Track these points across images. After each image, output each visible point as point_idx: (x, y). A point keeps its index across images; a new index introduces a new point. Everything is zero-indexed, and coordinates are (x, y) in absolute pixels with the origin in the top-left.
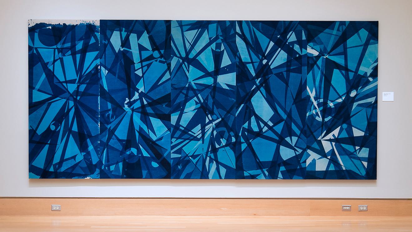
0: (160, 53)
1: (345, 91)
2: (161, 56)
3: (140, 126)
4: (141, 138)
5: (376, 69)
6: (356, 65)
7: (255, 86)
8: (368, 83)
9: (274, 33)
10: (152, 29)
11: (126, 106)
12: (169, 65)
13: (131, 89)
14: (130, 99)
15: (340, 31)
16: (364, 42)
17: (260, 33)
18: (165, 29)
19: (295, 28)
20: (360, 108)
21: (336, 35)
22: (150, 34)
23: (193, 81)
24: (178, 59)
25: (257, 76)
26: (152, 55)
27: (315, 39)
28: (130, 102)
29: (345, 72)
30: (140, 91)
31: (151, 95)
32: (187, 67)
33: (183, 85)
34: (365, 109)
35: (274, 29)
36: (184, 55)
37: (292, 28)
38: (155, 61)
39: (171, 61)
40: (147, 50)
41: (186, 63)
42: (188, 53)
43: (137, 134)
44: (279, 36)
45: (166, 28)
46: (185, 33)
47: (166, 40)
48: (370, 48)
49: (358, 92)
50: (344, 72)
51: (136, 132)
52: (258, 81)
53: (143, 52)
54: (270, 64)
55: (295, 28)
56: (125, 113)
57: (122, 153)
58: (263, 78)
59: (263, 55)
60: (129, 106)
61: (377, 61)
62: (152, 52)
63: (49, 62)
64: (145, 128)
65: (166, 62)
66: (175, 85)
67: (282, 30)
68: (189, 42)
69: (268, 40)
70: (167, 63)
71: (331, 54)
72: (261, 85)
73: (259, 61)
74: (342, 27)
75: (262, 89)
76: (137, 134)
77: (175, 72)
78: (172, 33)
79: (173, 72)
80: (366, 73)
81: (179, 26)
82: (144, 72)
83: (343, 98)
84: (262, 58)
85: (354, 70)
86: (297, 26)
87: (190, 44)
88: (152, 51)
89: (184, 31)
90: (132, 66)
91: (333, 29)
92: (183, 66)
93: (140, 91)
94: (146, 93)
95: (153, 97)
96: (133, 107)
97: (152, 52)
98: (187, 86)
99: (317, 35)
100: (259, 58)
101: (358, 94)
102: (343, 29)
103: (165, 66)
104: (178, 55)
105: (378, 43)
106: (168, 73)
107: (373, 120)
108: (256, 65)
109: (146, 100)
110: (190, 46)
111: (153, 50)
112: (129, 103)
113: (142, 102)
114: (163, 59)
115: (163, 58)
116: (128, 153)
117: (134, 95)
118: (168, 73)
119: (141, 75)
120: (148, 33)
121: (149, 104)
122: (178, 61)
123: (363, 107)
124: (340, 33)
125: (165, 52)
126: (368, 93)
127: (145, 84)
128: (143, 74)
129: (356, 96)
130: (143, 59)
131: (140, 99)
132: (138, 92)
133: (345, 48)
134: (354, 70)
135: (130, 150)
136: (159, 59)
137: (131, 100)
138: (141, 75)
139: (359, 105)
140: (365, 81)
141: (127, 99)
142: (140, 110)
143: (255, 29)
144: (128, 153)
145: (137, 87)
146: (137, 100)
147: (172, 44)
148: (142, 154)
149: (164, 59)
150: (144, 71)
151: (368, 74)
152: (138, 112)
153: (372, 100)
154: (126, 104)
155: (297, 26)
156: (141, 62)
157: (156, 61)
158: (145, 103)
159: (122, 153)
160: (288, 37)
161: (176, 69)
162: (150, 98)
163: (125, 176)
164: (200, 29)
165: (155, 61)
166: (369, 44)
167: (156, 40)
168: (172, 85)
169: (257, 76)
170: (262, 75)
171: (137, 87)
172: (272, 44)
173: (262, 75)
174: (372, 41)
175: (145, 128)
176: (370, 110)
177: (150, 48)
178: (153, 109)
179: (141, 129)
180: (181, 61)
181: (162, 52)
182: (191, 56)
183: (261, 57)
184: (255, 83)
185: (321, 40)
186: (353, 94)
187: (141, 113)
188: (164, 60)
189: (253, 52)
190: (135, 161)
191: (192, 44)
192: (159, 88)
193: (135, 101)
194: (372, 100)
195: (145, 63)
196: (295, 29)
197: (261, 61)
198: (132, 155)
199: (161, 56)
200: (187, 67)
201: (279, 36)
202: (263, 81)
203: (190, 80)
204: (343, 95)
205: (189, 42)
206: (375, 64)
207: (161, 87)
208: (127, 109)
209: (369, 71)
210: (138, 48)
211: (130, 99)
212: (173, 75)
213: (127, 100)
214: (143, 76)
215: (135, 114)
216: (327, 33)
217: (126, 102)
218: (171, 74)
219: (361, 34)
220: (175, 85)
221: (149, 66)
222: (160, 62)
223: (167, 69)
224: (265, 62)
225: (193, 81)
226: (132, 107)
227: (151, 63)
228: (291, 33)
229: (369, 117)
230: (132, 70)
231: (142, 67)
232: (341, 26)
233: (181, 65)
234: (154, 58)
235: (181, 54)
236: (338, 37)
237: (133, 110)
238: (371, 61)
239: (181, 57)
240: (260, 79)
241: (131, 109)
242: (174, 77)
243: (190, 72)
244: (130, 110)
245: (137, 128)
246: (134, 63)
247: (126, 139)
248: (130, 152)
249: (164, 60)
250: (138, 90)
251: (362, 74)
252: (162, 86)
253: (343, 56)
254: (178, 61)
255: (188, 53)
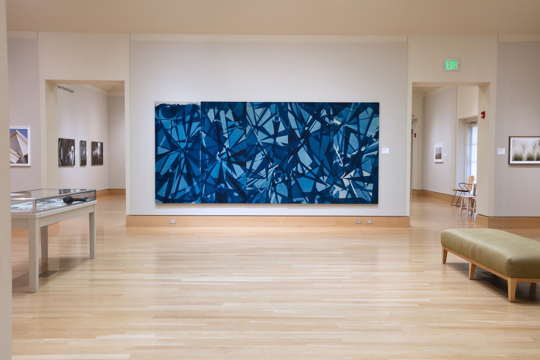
0: (239, 123)
3: (226, 170)
5: (377, 133)
7: (300, 144)
8: (372, 142)
11: (218, 157)
12: (245, 131)
13: (221, 146)
14: (220, 152)
21: (352, 112)
22: (233, 111)
23: (261, 140)
25: (302, 138)
26: (234, 124)
27: (339, 114)
30: (226, 148)
31: (234, 150)
33: (254, 143)
36: (254, 124)
40: (230, 121)
41: (256, 130)
42: (257, 123)
43: (225, 175)
44: (315, 112)
46: (256, 110)
48: (374, 120)
51: (224, 173)
52: (302, 141)
54: (310, 130)
56: (217, 161)
57: (215, 186)
59: (305, 124)
60: (220, 157)
61: (378, 128)
64: (230, 171)
65: (243, 129)
67: (318, 108)
71: (349, 123)
72: (304, 143)
73: (302, 128)
74: (356, 107)
75: (305, 146)
76: (225, 175)
77: (249, 135)
78: (247, 110)
80: (371, 136)
83: (357, 152)
85: (364, 134)
86: (327, 106)
87: (259, 117)
90: (221, 131)
92: (254, 131)
93: (226, 148)
98: (257, 144)
100: (303, 126)
103: (243, 131)
104: (251, 124)
105: (379, 116)
106: (244, 135)
107: (375, 166)
108: (301, 130)
111: (235, 121)
113: (228, 154)
114: (241, 127)
116: (219, 187)
118: (244, 135)
119: (227, 137)
121: (232, 156)
122: (251, 128)
123: (370, 157)
124: (355, 110)
125: (242, 122)
128: (229, 136)
129: (365, 150)
130: (228, 127)
131: (227, 152)
132: (225, 148)
133: (358, 120)
135: (220, 185)
136: (239, 127)
137: (221, 153)
138: (227, 137)
139: (367, 156)
141: (218, 152)
142: (227, 160)
143: (300, 108)
144: (219, 187)
145: (225, 144)
147: (247, 117)
148: (228, 187)
150: (229, 135)
151: (373, 137)
153: (375, 153)
154: (218, 155)
155: (327, 106)
156: (227, 128)
157: (237, 128)
158: (230, 155)
159: (215, 186)
161: (250, 133)
163: (217, 202)
164: (265, 108)
168: (247, 143)
169: (302, 138)
172: (311, 117)
174: (375, 115)
175: (230, 171)
176: (374, 159)
179: (227, 171)
180: (253, 128)
181: (241, 122)
182: (259, 125)
183: (304, 125)
184: (300, 143)
186: (363, 149)
188: (242, 128)
190: (223, 192)
193: (223, 154)
194: (375, 153)
195: (229, 130)
197: (304, 128)
199: (240, 125)
201: (315, 112)
203: (259, 140)
204: (356, 150)
206: (377, 130)
207: (240, 145)
209: (373, 135)
211: (220, 152)
213: (218, 153)
214: (228, 138)
216: (346, 110)
217: (217, 154)
218: (246, 136)
221: (232, 131)
222: (240, 128)
224: (306, 128)
225: (261, 140)
226: (221, 157)
227: (234, 129)
228: (323, 110)
229: (373, 164)
231: (228, 132)
233: (253, 131)
237: (222, 159)
238: (374, 128)
239: (253, 126)
240: (303, 140)
242: (248, 138)
244: (220, 160)
245: (225, 171)
249: (242, 128)
250: (225, 147)
251: (369, 136)
252: (241, 144)
253: (357, 125)
255: (257, 123)
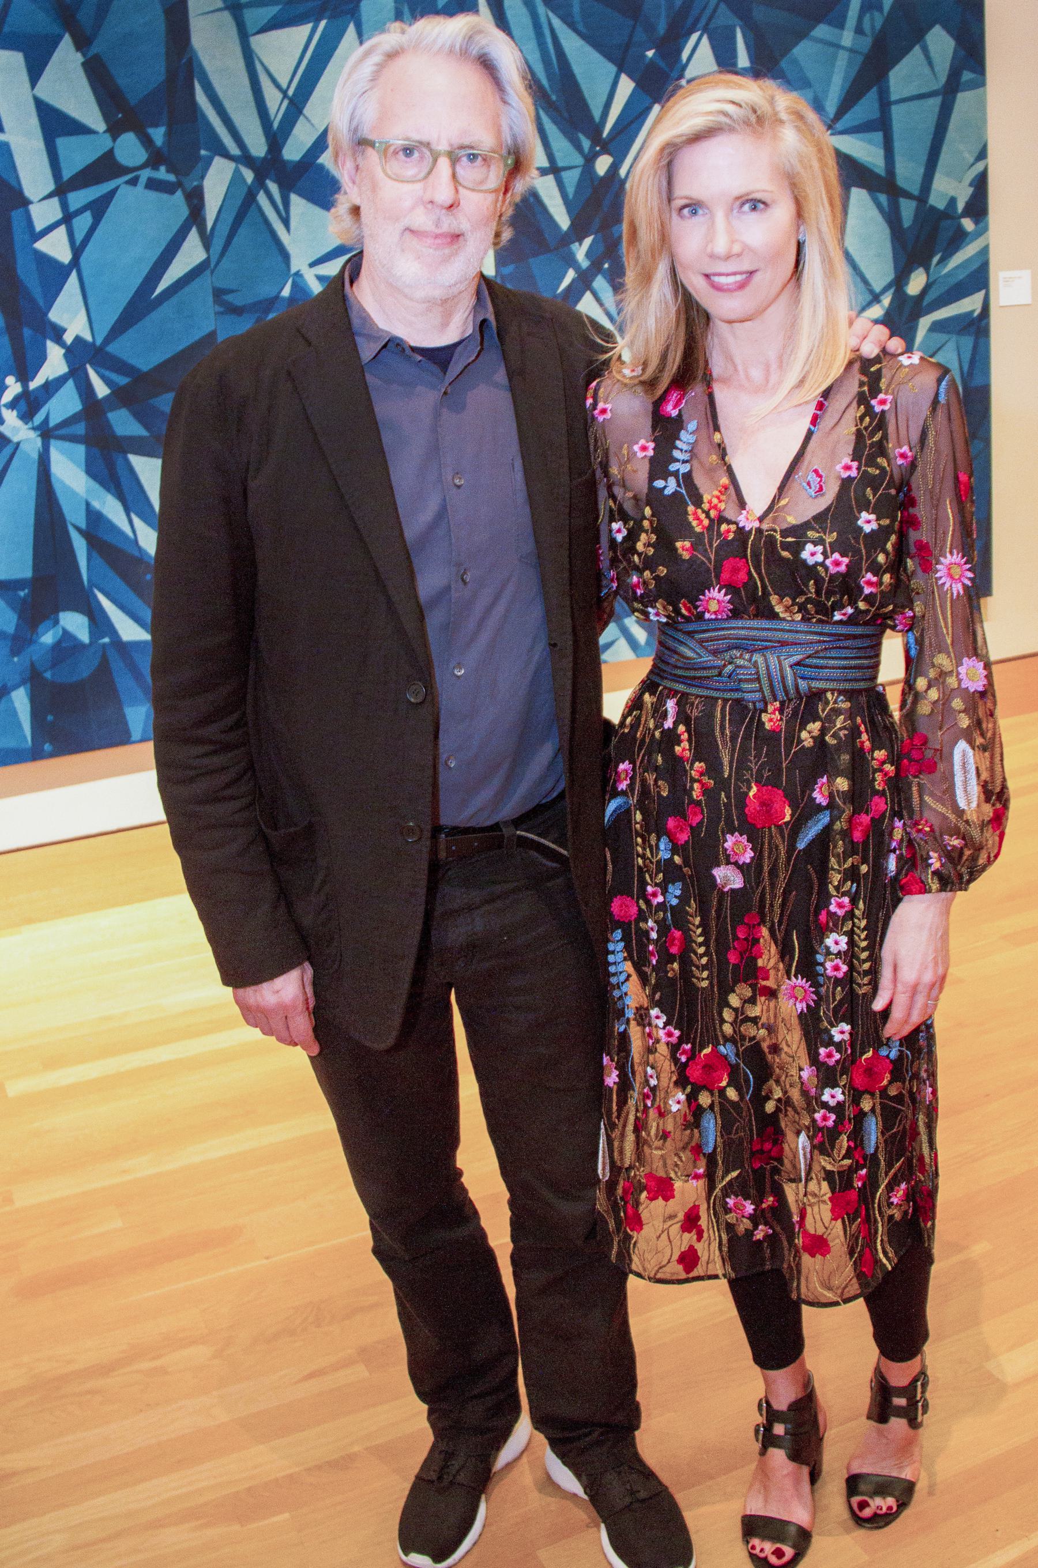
0: (147, 141)
1: (890, 276)
2: (156, 159)
3: (88, 504)
4: (98, 560)
5: (981, 183)
6: (922, 170)
7: (571, 275)
8: (959, 238)
9: (631, 36)
10: (98, 25)
11: (11, 417)
12: (196, 199)
13: (27, 332)
14: (24, 377)
15: (866, 35)
16: (943, 79)
17: (574, 36)
18: (160, 25)
19: (710, 19)
20: (942, 337)
21: (851, 50)
22: (90, 54)
23: (312, 265)
24: (237, 171)
25: (578, 232)
26: (110, 154)
27: (784, 64)
28: (25, 394)
29: (889, 200)
30: (69, 338)
31: (122, 348)
32: (281, 207)
33: (265, 291)
34: (954, 338)
35: (632, 23)
36: (258, 147)
37: (697, 20)
38: (127, 182)
39: (203, 177)
40: (78, 129)
41: (273, 187)
42: (276, 139)
43: (80, 545)
44: (650, 54)
45: (162, 18)
46: (258, 42)
47: (172, 75)
48: (964, 100)
49: (931, 276)
50: (883, 198)
51: (75, 536)
52: (581, 251)
53: (63, 143)
54: (623, 172)
55: (710, 19)
56: (7, 451)
57: (20, 642)
58: (600, 235)
59: (594, 131)
60: (26, 417)
61: (982, 155)
62: (105, 142)
63: (445, 374)
64: (112, 509)
65: (179, 185)
66: (232, 291)
67: (662, 28)
68: (278, 86)
69: (613, 69)
70: (184, 191)
71: (839, 126)
72: (596, 267)
73: (579, 160)
74: (872, 19)
75: (600, 283)
76: (80, 545)
77: (224, 230)
78: (197, 41)
79: (216, 233)
80: (953, 201)
81: (227, 8)
82: (78, 242)
83: (886, 300)
84: (592, 148)
85: (916, 193)
86: (715, 10)
87: (285, 93)
88: (108, 135)
89: (251, 30)
90: (16, 215)
91: (841, 25)
92: (262, 199)
93: (69, 338)
94: (99, 342)
95: (134, 361)
96: (46, 420)
97: (105, 142)
98: (286, 292)
99: (787, 50)
100: (578, 147)
101: (934, 282)
102: (873, 27)
103: (177, 205)
104: (234, 150)
105: (983, 84)
106: (193, 237)
107: (977, 381)
108: (571, 178)
109: (103, 377)
110: (286, 103)
111: (115, 130)
112: (23, 403)
113: (86, 390)
114: (162, 174)
115: (163, 169)
116: (48, 638)
117: (42, 358)
118: (193, 237)
119: (64, 256)
120: (81, 44)
121: (121, 397)
122: (237, 174)
123: (949, 332)
124: (866, 43)
125: (169, 134)
126: (961, 276)
127: (90, 301)
128: (77, 252)
129: (924, 292)
130: (67, 174)
131: (76, 372)
132: (58, 339)
133: (885, 104)
134: (916, 193)
135: (57, 622)
136: (145, 174)
137: (33, 385)
138: (64, 256)
139: (937, 327)
140: (950, 234)
141: (10, 380)
142: (80, 429)
143: (556, 22)
144: (48, 638)
145: (54, 316)
146: (61, 381)
147: (201, 98)
148: (113, 632)
149: (168, 171)
150: (79, 237)
151: (960, 206)
152: (73, 439)
153: (971, 304)
154: (12, 405)
155: (715, 10)
156: (61, 191)
157: (134, 182)
158: (102, 390)
160: (685, 56)
161: (229, 218)
162: (121, 366)
163: (47, 747)
164: (323, 23)
165: (127, 182)
166: (958, 86)
167: (122, 80)
168: (218, 294)
169: (578, 232)
170: (597, 223)
171: (54, 316)
172: (626, 86)
173: (597, 223)
174: (967, 76)
175: (112, 509)
176: (967, 342)
177: (99, 124)
178: (141, 417)
179: (95, 517)
180: (249, 176)
181: (158, 135)
182: (293, 152)
183: (586, 144)
184: (570, 261)
185: (801, 69)
186: (916, 284)
187: (86, 440)
188: (172, 178)
189: (555, 122)
190: (85, 669)
191: (291, 92)
192: (155, 316)
193: (51, 388)
194: (971, 304)
195: (78, 199)
196: (707, 24)
197: (590, 160)
198: (67, 646)
199: (156, 159)
200: (281, 207)
201: (650, 54)
202: (601, 248)
203: (299, 263)
204: (885, 290)
205: (278, 86)
206: (980, 167)
207: (166, 310)
208: (16, 430)
209: (963, 195)
210: (34, 121)
211: (24, 377)
212: (218, 244)
213: (13, 387)
214: (75, 262)
215: (62, 452)
216: (821, 41)
217: (8, 396)
218: (207, 241)
219: (932, 48)
220: (232, 291)
221: (99, 208)
222: (153, 185)
223: (187, 219)
224: (603, 164)
225: (312, 265)
226: (39, 419)
227: (112, 193)
228: (695, 37)
229: (966, 368)
230: (19, 235)
231: (67, 219)
232: (868, 15)
233: (250, 198)
234: (124, 170)
235: (248, 140)
236: (860, 59)
237: (47, 433)
238: (967, 155)
239: (246, 159)
240: (588, 241)
241: (34, 429)
242: (223, 254)
243: (293, 223)
244: (33, 435)
245: (75, 516)
246: (25, 202)
247: (28, 573)
248: (54, 636)
249: (172, 178)
250: (57, 332)
251: (941, 205)
252: (174, 300)
253: (879, 136)
254: (237, 178)
255: (276, 139)
